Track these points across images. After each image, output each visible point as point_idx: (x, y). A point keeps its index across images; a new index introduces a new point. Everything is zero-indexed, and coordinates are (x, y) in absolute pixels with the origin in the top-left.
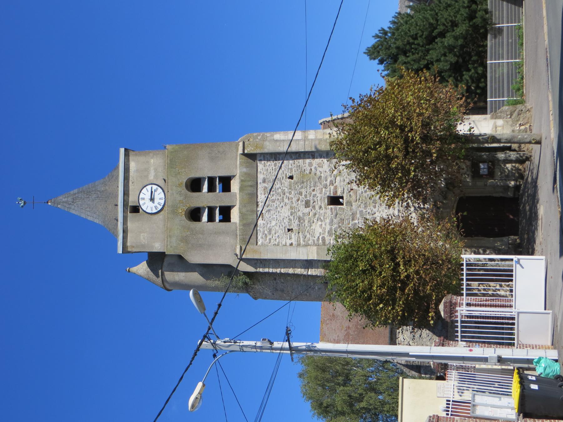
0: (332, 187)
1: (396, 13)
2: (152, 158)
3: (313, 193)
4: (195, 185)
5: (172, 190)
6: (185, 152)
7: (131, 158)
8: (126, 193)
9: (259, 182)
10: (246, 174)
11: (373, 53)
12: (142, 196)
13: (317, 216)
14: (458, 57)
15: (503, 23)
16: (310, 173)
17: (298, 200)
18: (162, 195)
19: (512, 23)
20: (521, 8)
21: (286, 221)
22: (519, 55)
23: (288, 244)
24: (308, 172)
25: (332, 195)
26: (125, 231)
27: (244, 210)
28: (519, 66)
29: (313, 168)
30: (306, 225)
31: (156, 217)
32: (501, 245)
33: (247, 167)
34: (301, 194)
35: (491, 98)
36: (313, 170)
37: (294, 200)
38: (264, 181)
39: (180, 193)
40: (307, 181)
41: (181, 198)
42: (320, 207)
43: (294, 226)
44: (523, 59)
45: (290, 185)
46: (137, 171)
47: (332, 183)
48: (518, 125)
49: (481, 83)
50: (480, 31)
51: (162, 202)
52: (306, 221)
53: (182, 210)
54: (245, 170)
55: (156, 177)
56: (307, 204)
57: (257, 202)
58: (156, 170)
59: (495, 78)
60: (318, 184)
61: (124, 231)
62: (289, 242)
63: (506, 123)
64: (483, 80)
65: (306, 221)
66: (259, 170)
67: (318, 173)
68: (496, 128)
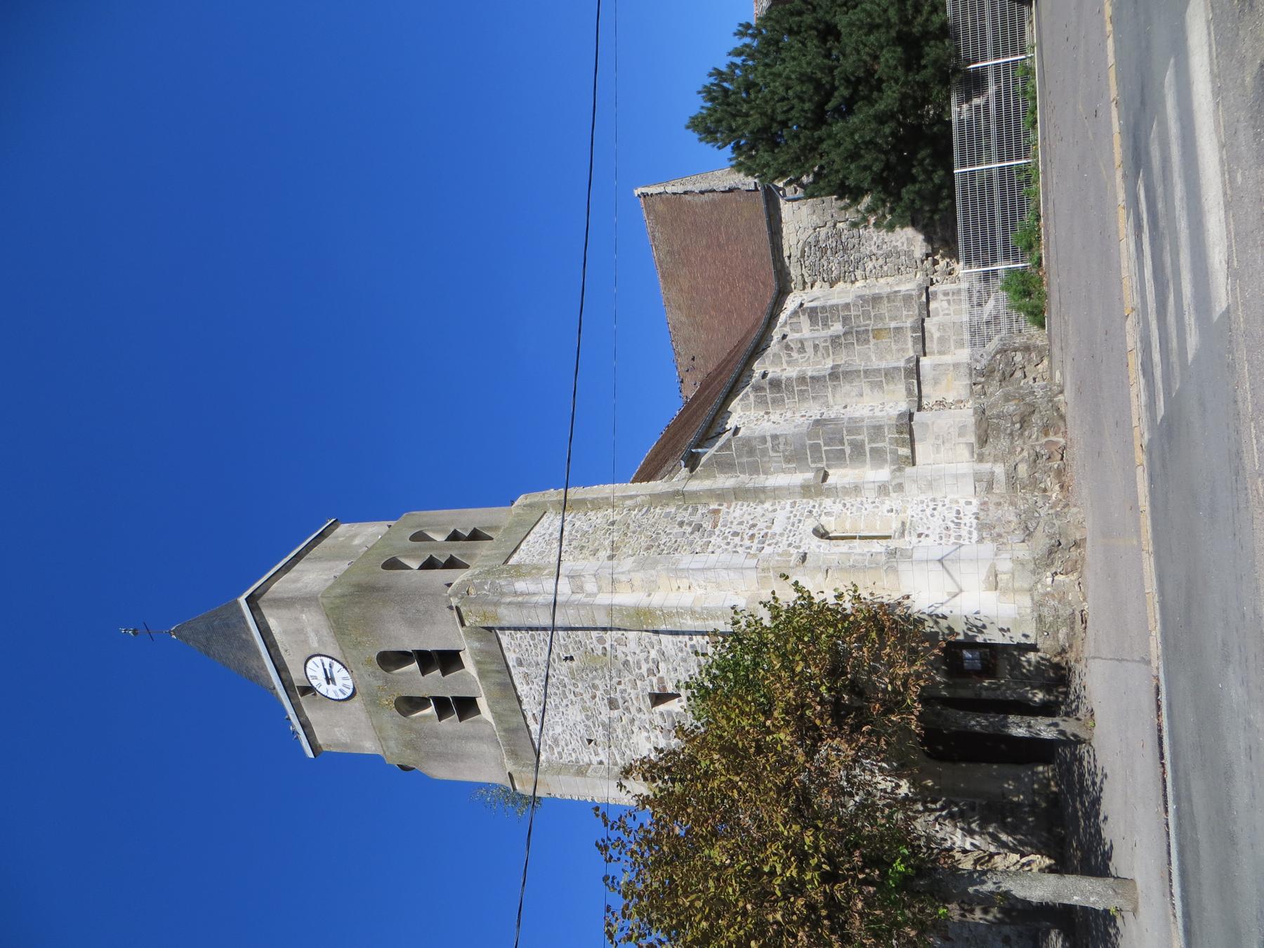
0: (655, 680)
1: (741, 25)
2: (302, 612)
3: (619, 687)
4: (391, 660)
5: (357, 669)
6: (356, 610)
7: (266, 612)
8: (281, 668)
9: (510, 665)
10: (481, 651)
11: (707, 128)
12: (310, 673)
13: (637, 723)
14: (886, 153)
15: (984, 59)
16: (605, 655)
17: (594, 697)
18: (344, 673)
19: (1010, 159)
20: (1026, 9)
21: (581, 727)
22: (1027, 149)
23: (595, 762)
24: (600, 653)
25: (657, 691)
26: (306, 725)
27: (498, 708)
28: (1028, 177)
29: (607, 646)
30: (620, 736)
31: (348, 704)
32: (1017, 792)
33: (480, 640)
34: (595, 687)
35: (963, 166)
36: (609, 649)
37: (587, 697)
38: (520, 663)
39: (373, 674)
40: (602, 668)
41: (380, 683)
42: (640, 710)
43: (599, 734)
44: (1035, 156)
45: (572, 673)
46: (285, 632)
47: (650, 672)
48: (1049, 574)
49: (943, 199)
50: (930, 59)
51: (350, 683)
52: (619, 731)
53: (388, 700)
54: (477, 644)
55: (320, 641)
56: (612, 704)
57: (518, 697)
58: (317, 632)
59: (973, 188)
60: (626, 673)
61: (303, 727)
62: (595, 760)
63: (1020, 567)
64: (945, 193)
65: (619, 731)
66: (504, 645)
67: (621, 656)
68: (996, 576)
